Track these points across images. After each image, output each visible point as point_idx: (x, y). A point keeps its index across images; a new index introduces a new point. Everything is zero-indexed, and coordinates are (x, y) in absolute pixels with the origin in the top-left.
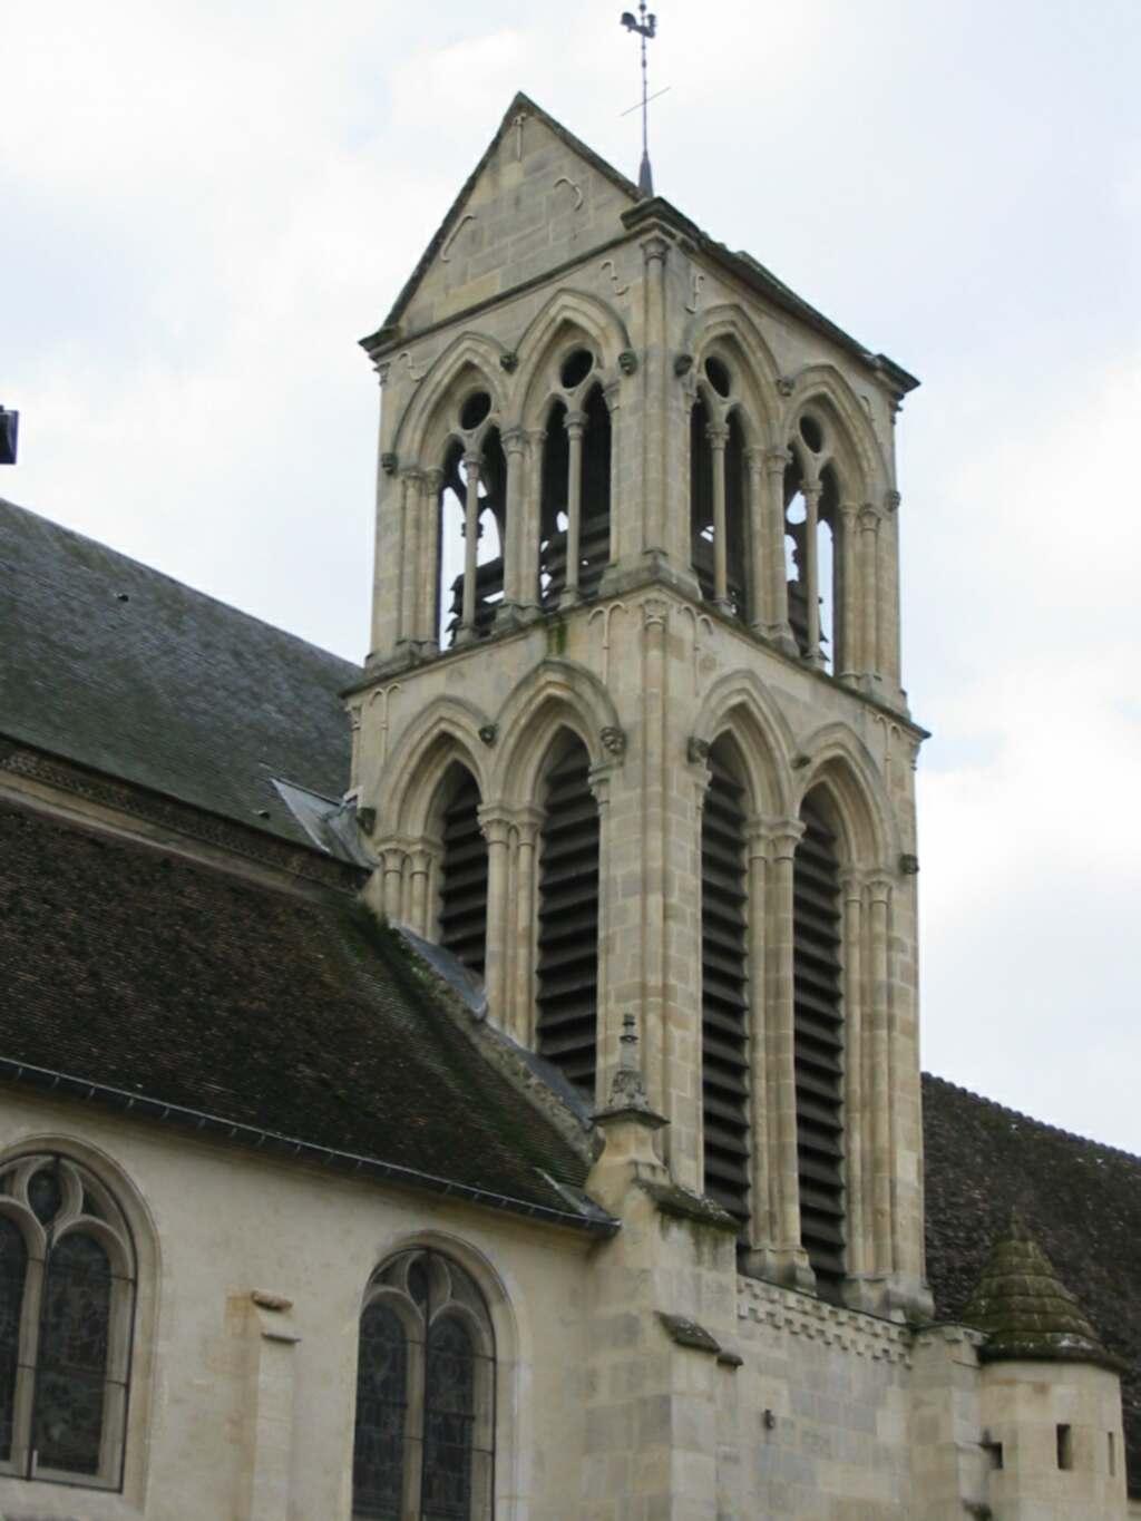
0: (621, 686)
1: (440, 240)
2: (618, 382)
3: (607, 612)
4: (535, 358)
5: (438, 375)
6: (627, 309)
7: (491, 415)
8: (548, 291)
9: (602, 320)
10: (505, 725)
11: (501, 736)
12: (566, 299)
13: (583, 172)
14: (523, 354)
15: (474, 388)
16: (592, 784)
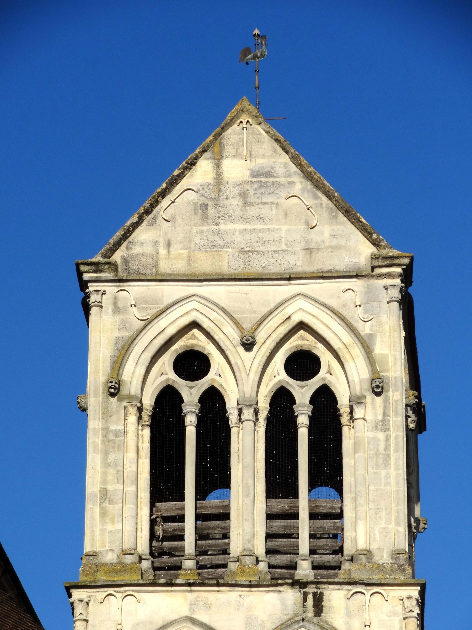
1: (160, 199)
2: (365, 397)
3: (368, 594)
4: (270, 344)
5: (163, 322)
6: (371, 336)
7: (211, 375)
9: (347, 337)
12: (301, 303)
13: (316, 197)
14: (260, 336)
15: (193, 345)
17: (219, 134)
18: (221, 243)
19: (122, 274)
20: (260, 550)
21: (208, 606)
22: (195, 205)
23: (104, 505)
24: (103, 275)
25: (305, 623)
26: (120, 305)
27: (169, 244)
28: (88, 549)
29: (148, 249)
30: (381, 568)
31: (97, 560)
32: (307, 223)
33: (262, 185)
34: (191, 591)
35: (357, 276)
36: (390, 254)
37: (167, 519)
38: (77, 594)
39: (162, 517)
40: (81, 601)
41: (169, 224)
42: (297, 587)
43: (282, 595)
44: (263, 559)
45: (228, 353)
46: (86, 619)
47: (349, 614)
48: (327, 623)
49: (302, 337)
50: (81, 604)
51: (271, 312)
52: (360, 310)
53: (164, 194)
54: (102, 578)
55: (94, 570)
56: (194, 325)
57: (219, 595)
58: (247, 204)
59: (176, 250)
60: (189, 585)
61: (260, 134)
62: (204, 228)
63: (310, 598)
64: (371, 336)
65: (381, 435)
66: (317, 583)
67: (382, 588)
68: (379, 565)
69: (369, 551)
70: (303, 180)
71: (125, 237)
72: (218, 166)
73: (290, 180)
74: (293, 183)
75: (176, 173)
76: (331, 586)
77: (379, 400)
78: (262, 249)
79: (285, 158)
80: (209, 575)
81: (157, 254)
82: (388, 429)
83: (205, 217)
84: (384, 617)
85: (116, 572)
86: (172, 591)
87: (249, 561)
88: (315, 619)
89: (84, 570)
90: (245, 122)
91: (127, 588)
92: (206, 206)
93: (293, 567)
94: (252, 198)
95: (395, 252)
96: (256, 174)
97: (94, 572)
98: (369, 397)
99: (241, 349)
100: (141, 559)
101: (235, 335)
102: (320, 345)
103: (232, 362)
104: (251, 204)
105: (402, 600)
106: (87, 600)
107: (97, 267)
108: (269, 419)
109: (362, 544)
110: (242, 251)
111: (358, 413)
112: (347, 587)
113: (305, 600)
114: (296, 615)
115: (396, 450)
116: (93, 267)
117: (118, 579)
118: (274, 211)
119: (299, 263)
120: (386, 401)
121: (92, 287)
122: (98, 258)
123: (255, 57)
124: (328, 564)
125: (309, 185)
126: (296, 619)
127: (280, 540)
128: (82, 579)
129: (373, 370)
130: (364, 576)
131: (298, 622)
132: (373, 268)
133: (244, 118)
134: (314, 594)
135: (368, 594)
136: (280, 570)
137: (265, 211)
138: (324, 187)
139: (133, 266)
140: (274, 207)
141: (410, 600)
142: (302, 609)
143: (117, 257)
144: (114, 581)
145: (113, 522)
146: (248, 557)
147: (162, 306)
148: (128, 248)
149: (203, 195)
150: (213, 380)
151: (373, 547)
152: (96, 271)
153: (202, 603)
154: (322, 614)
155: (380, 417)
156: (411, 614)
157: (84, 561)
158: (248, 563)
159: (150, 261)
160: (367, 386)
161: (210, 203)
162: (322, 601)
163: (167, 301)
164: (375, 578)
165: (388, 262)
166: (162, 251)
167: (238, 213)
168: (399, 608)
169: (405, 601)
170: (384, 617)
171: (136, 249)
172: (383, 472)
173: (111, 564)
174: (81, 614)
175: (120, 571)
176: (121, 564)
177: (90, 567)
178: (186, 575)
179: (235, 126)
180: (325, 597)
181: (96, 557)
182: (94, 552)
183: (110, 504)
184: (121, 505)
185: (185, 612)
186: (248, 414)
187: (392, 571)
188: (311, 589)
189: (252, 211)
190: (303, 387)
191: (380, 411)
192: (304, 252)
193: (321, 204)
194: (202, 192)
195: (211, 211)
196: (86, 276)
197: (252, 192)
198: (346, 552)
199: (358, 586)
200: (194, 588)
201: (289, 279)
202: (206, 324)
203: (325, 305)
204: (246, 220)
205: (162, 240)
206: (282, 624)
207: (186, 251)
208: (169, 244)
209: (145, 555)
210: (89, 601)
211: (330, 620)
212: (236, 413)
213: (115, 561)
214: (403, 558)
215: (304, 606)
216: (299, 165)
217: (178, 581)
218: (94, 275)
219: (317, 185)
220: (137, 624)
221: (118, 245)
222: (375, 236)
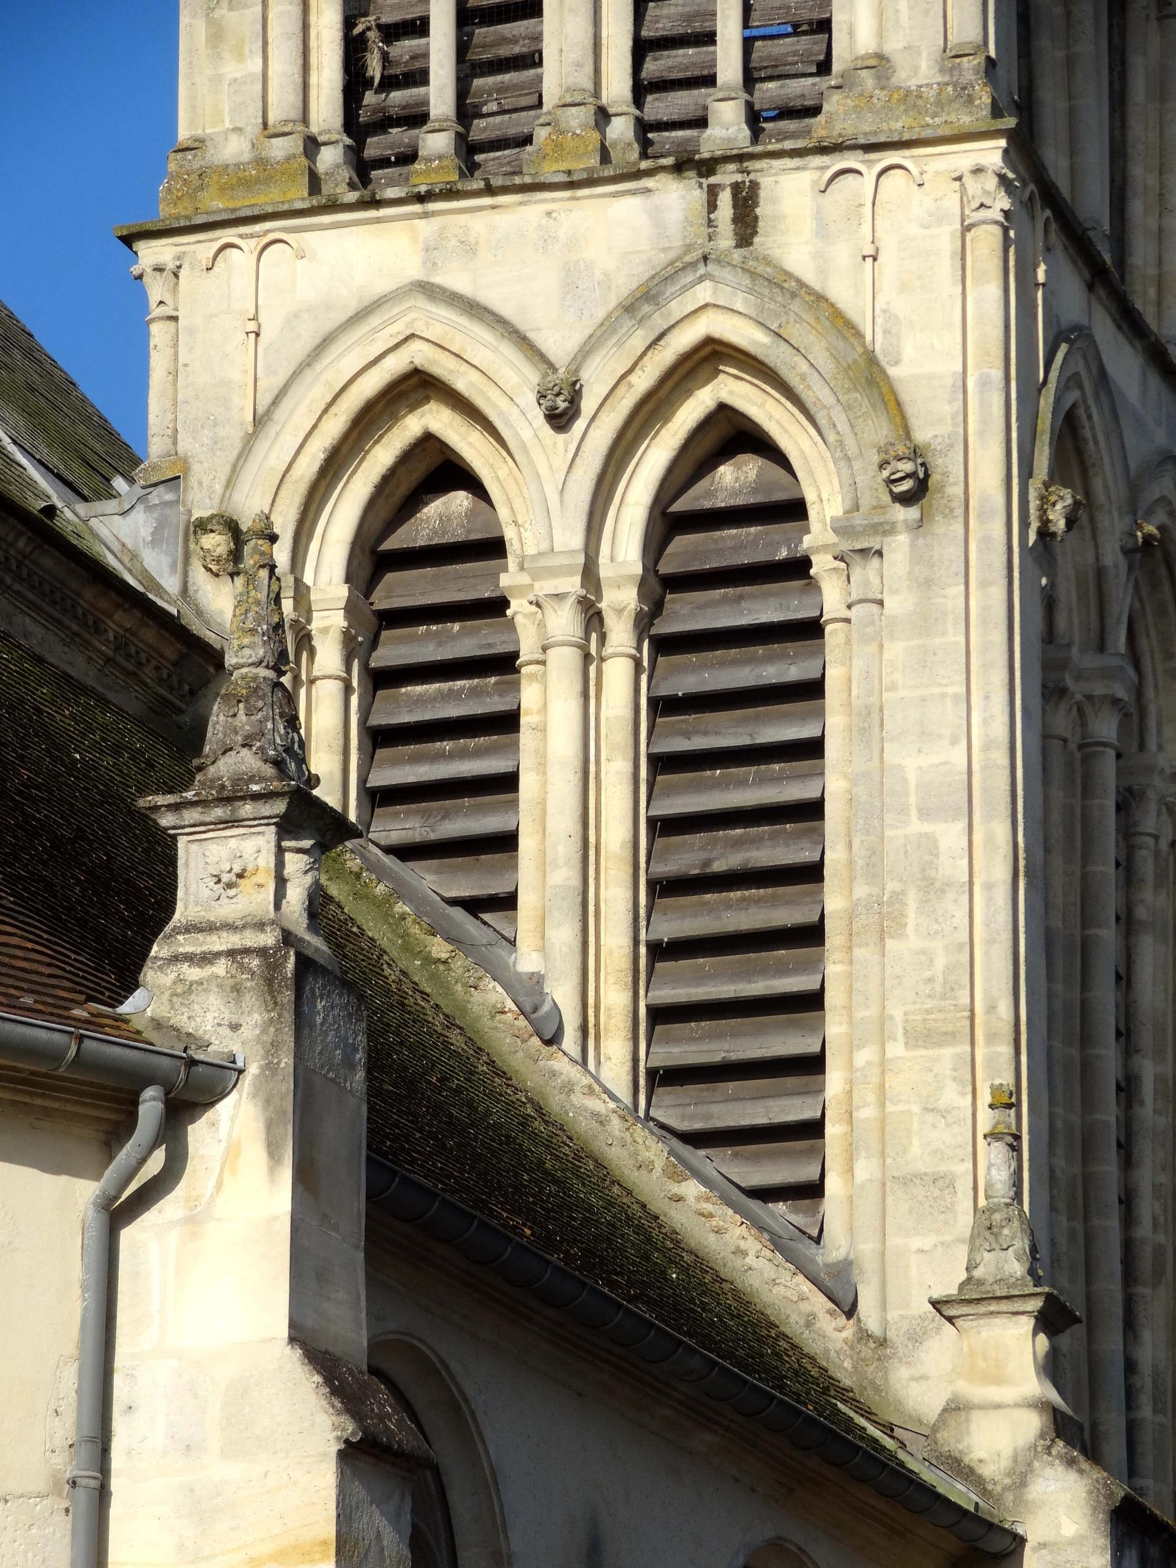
3: (870, 175)
11: (588, 405)
21: (469, 249)
23: (217, 14)
25: (711, 267)
28: (184, 133)
30: (911, 99)
31: (204, 158)
34: (426, 215)
37: (393, 32)
38: (151, 253)
39: (380, 27)
40: (159, 269)
42: (692, 173)
43: (655, 199)
44: (619, 110)
46: (174, 314)
47: (823, 230)
48: (767, 261)
50: (161, 276)
54: (216, 204)
55: (194, 187)
57: (497, 218)
60: (421, 199)
63: (725, 199)
66: (740, 158)
67: (907, 152)
68: (908, 92)
69: (880, 56)
76: (777, 163)
80: (501, 165)
84: (914, 230)
85: (247, 184)
86: (378, 221)
87: (578, 119)
88: (737, 255)
89: (169, 190)
91: (268, 225)
93: (701, 122)
97: (196, 190)
100: (312, 145)
105: (959, 179)
106: (171, 265)
112: (818, 160)
113: (712, 206)
114: (688, 248)
117: (246, 203)
124: (798, 103)
126: (688, 259)
127: (681, 52)
128: (166, 212)
130: (866, 127)
131: (692, 265)
134: (736, 188)
136: (674, 134)
141: (982, 176)
142: (705, 231)
144: (234, 210)
145: (240, 57)
146: (574, 110)
151: (893, 46)
153: (453, 242)
154: (756, 240)
156: (984, 214)
157: (172, 167)
158: (574, 123)
162: (756, 204)
164: (898, 125)
168: (952, 203)
169: (968, 180)
170: (914, 230)
173: (237, 165)
174: (161, 302)
175: (258, 181)
176: (261, 162)
177: (185, 180)
178: (427, 172)
180: (762, 194)
181: (199, 152)
182: (196, 141)
183: (231, 9)
184: (259, 8)
185: (412, 269)
187: (940, 104)
188: (727, 176)
198: (836, 67)
199: (847, 154)
200: (432, 206)
206: (653, 277)
209: (329, 131)
210: (179, 267)
211: (775, 253)
213: (246, 157)
214: (971, 66)
215: (710, 223)
217: (391, 193)
220: (296, 315)
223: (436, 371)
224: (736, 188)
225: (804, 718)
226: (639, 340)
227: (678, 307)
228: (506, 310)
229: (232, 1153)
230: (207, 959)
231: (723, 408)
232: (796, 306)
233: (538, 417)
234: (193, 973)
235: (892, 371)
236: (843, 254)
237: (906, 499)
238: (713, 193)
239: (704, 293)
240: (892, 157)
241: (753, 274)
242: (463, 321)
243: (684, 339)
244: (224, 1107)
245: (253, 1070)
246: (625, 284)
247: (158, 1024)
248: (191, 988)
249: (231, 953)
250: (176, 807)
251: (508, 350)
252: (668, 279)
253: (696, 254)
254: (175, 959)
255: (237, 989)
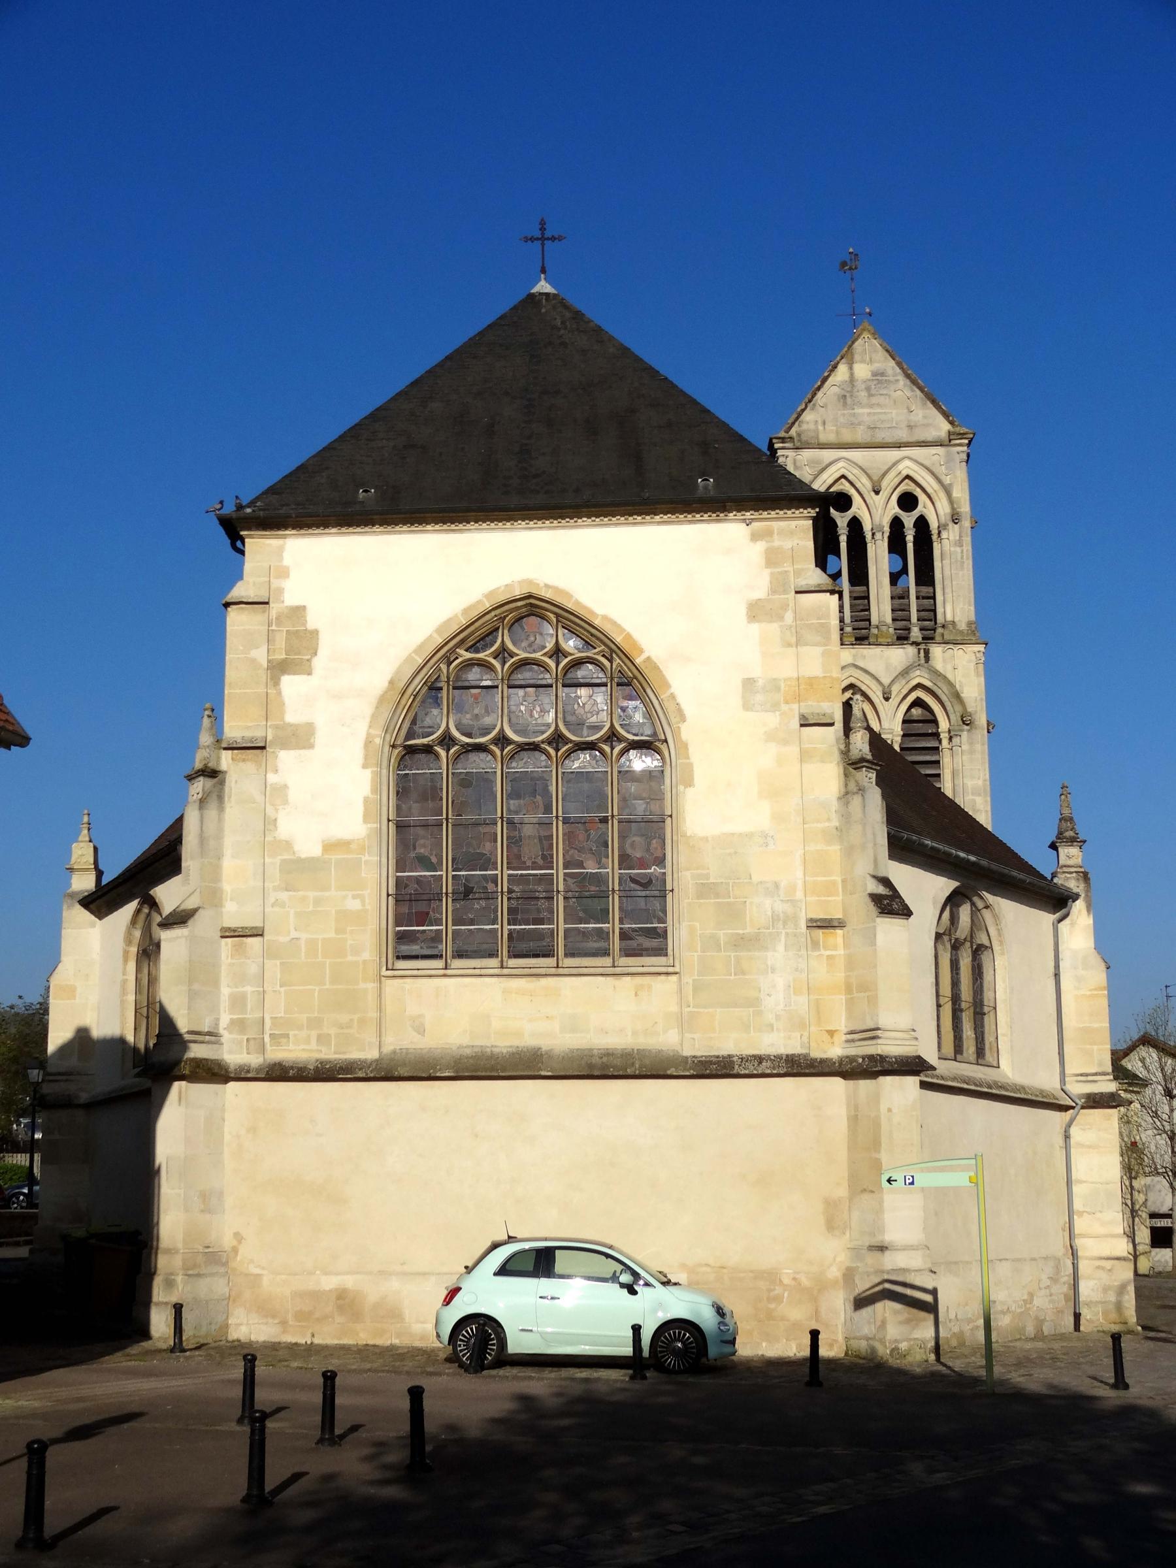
0: (965, 691)
4: (889, 490)
8: (895, 454)
10: (895, 689)
12: (907, 463)
13: (913, 391)
14: (884, 484)
16: (943, 732)
17: (850, 346)
18: (856, 422)
19: (798, 444)
20: (889, 619)
22: (838, 395)
24: (786, 445)
26: (798, 464)
27: (824, 423)
29: (812, 426)
32: (908, 408)
33: (880, 382)
35: (941, 445)
36: (962, 432)
41: (823, 409)
45: (864, 496)
47: (944, 661)
48: (932, 667)
49: (907, 484)
51: (890, 469)
52: (943, 467)
53: (819, 389)
56: (843, 477)
57: (870, 650)
58: (870, 395)
59: (830, 427)
61: (876, 346)
62: (845, 412)
63: (922, 651)
64: (950, 485)
65: (958, 549)
70: (905, 379)
71: (797, 418)
72: (851, 368)
73: (896, 378)
74: (897, 381)
75: (826, 374)
77: (956, 526)
78: (882, 426)
79: (892, 363)
81: (818, 429)
82: (962, 546)
83: (845, 404)
84: (965, 663)
90: (866, 337)
92: (845, 396)
93: (909, 629)
94: (873, 392)
95: (965, 430)
96: (875, 374)
98: (951, 524)
99: (873, 494)
101: (869, 485)
102: (918, 490)
103: (868, 502)
104: (872, 395)
107: (783, 440)
108: (889, 537)
109: (949, 617)
110: (869, 428)
111: (944, 535)
113: (919, 653)
114: (914, 662)
115: (968, 559)
116: (780, 440)
118: (887, 401)
119: (904, 436)
120: (960, 528)
121: (780, 453)
122: (782, 434)
123: (850, 269)
125: (908, 382)
129: (953, 508)
132: (950, 441)
133: (866, 335)
134: (925, 649)
135: (955, 649)
137: (881, 400)
138: (918, 383)
139: (804, 438)
140: (887, 397)
143: (793, 432)
147: (824, 465)
148: (799, 426)
149: (843, 389)
150: (856, 512)
152: (783, 443)
155: (958, 538)
159: (813, 434)
160: (949, 518)
161: (848, 395)
163: (827, 462)
165: (959, 437)
166: (821, 428)
167: (865, 401)
171: (805, 427)
172: (961, 573)
179: (860, 340)
185: (850, 660)
186: (878, 536)
187: (968, 635)
188: (922, 646)
189: (874, 400)
190: (909, 517)
191: (958, 534)
192: (907, 428)
193: (916, 396)
194: (842, 387)
195: (849, 400)
196: (776, 446)
197: (873, 387)
201: (900, 447)
202: (851, 477)
203: (922, 465)
204: (871, 406)
205: (820, 422)
207: (835, 428)
208: (824, 423)
211: (934, 665)
212: (870, 534)
216: (902, 368)
218: (781, 445)
219: (914, 382)
221: (793, 423)
222: (951, 418)
223: (857, 684)
224: (925, 649)
225: (935, 768)
226: (904, 682)
227: (912, 675)
228: (873, 672)
229: (1080, 911)
230: (1072, 873)
231: (918, 698)
232: (939, 678)
233: (882, 699)
234: (1068, 875)
235: (962, 695)
236: (949, 667)
237: (967, 725)
238: (919, 650)
239: (918, 673)
240: (960, 646)
241: (930, 670)
242: (864, 674)
243: (914, 682)
244: (1077, 902)
245: (1083, 895)
246: (900, 669)
247: (1062, 885)
248: (1068, 878)
249: (1076, 872)
250: (1060, 842)
251: (874, 682)
252: (911, 669)
253: (917, 664)
254: (1064, 872)
255: (1078, 879)
